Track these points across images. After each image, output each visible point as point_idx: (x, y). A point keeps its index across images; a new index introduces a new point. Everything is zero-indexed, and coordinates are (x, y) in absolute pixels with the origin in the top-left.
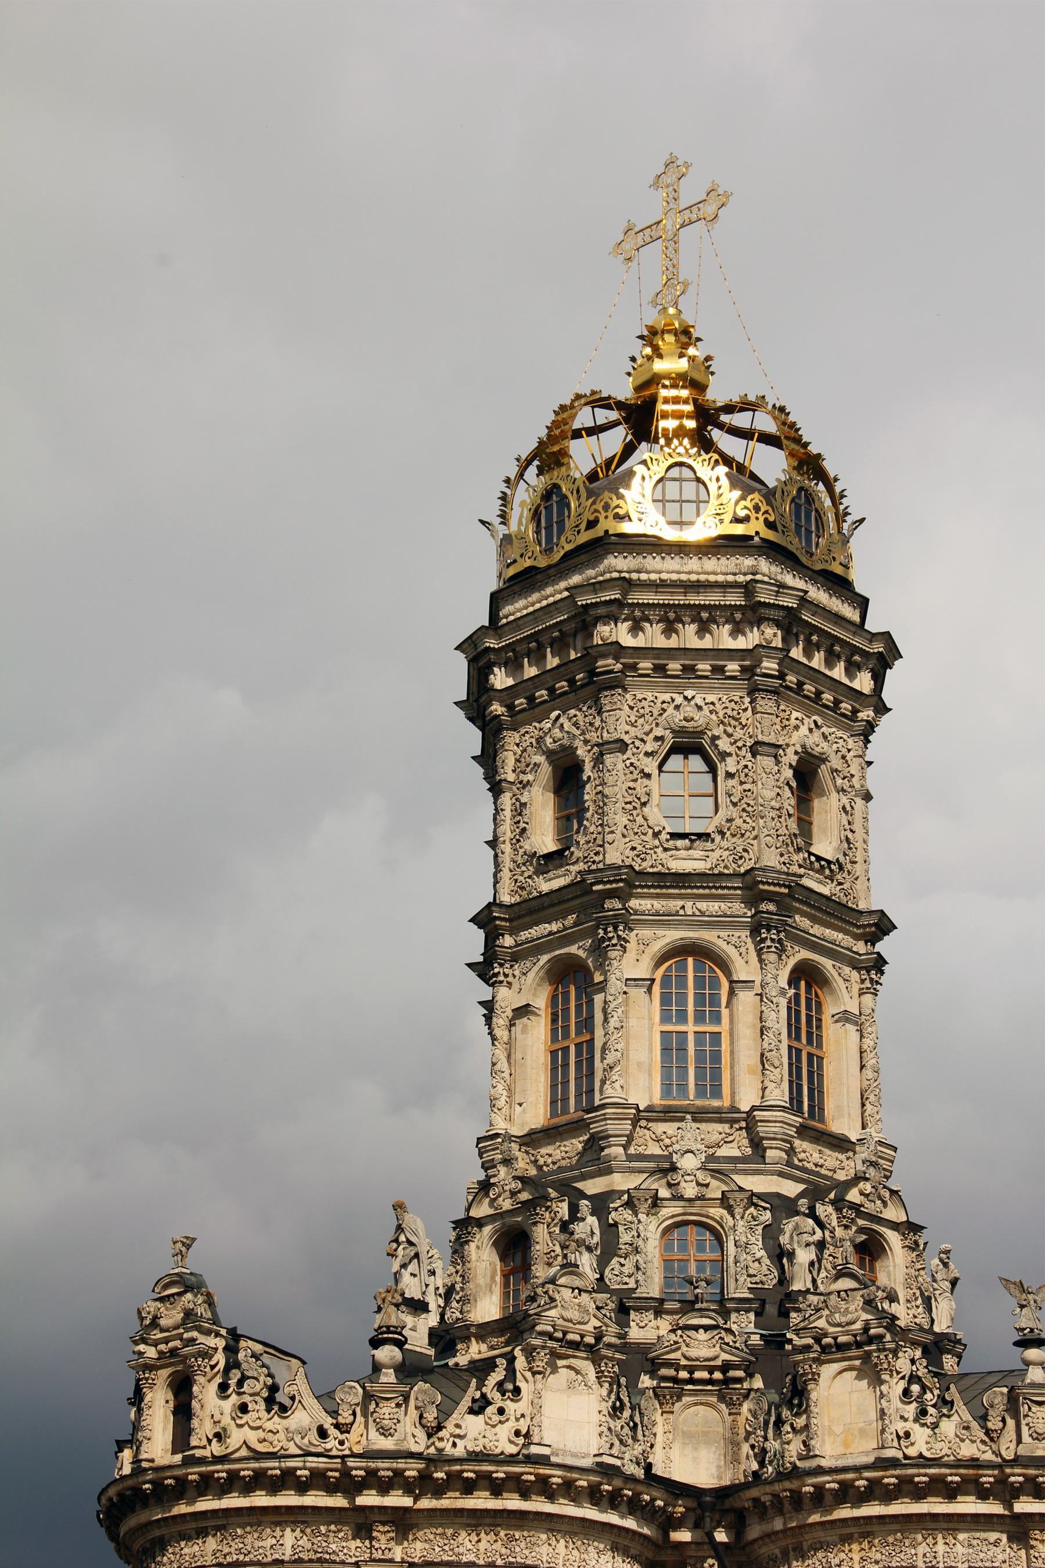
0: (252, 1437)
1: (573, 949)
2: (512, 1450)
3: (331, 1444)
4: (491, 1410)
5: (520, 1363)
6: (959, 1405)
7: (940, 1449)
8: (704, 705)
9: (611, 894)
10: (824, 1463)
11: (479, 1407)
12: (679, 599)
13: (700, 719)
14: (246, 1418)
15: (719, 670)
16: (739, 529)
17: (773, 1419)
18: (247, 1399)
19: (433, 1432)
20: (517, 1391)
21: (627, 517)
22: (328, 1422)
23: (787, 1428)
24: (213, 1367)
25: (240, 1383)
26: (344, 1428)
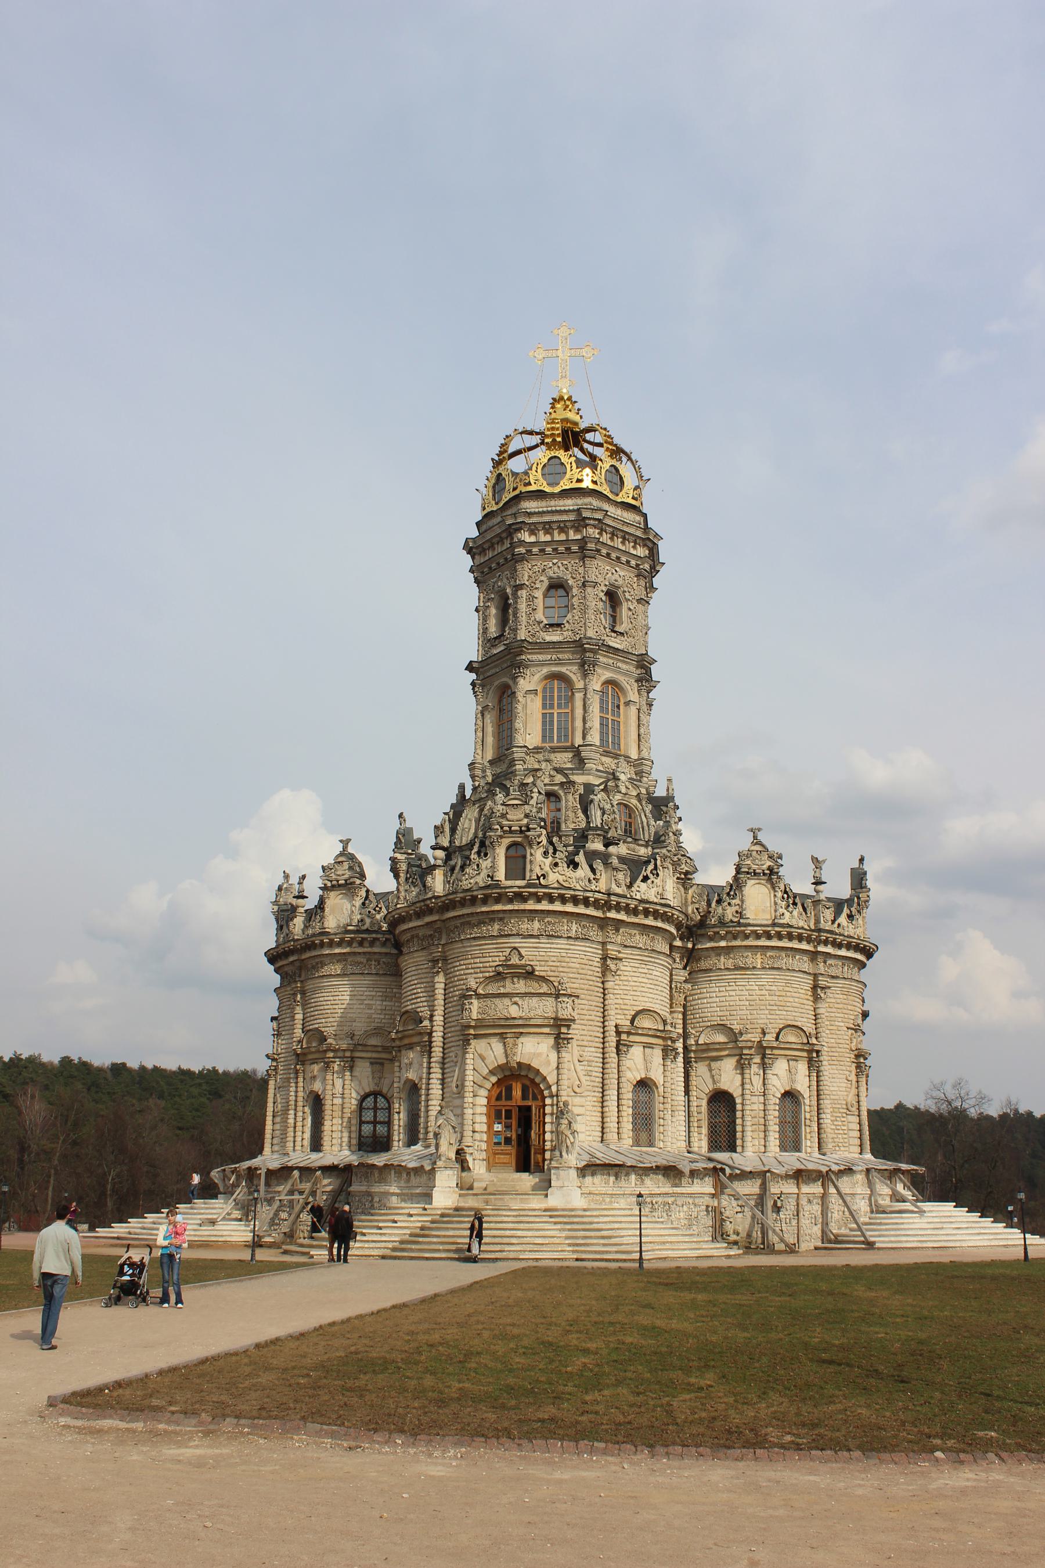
0: (561, 879)
1: (563, 669)
2: (656, 900)
3: (594, 887)
4: (649, 881)
5: (659, 863)
6: (799, 905)
7: (794, 923)
8: (622, 577)
9: (591, 651)
10: (751, 922)
11: (646, 879)
12: (620, 527)
13: (620, 582)
14: (559, 869)
15: (628, 562)
16: (633, 502)
17: (716, 898)
18: (557, 860)
19: (630, 886)
20: (658, 875)
21: (595, 482)
22: (592, 876)
23: (726, 904)
24: (539, 843)
25: (554, 853)
26: (597, 880)
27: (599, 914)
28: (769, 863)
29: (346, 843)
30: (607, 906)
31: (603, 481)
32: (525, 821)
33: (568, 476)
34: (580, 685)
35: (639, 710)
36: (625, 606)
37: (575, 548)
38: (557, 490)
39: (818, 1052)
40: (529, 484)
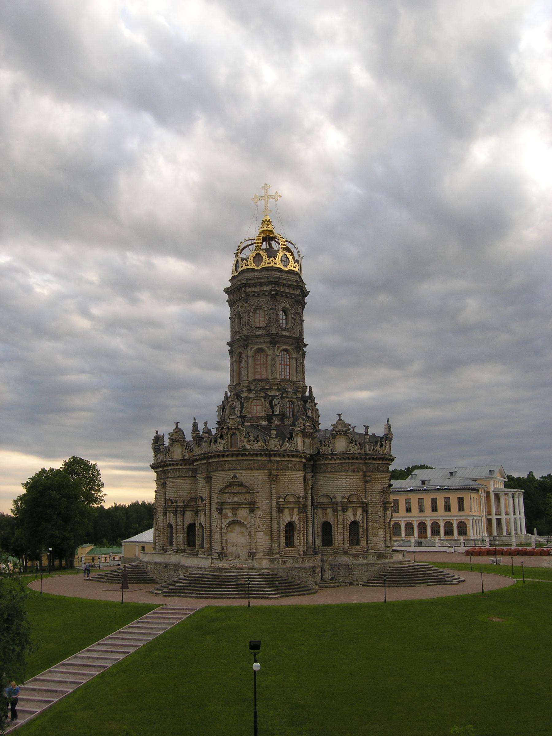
1: (263, 346)
21: (276, 264)
27: (268, 459)
28: (345, 429)
29: (177, 424)
30: (270, 455)
31: (280, 262)
32: (237, 425)
33: (264, 261)
34: (270, 352)
35: (296, 360)
36: (290, 315)
37: (267, 293)
38: (260, 267)
39: (366, 504)
40: (248, 265)
